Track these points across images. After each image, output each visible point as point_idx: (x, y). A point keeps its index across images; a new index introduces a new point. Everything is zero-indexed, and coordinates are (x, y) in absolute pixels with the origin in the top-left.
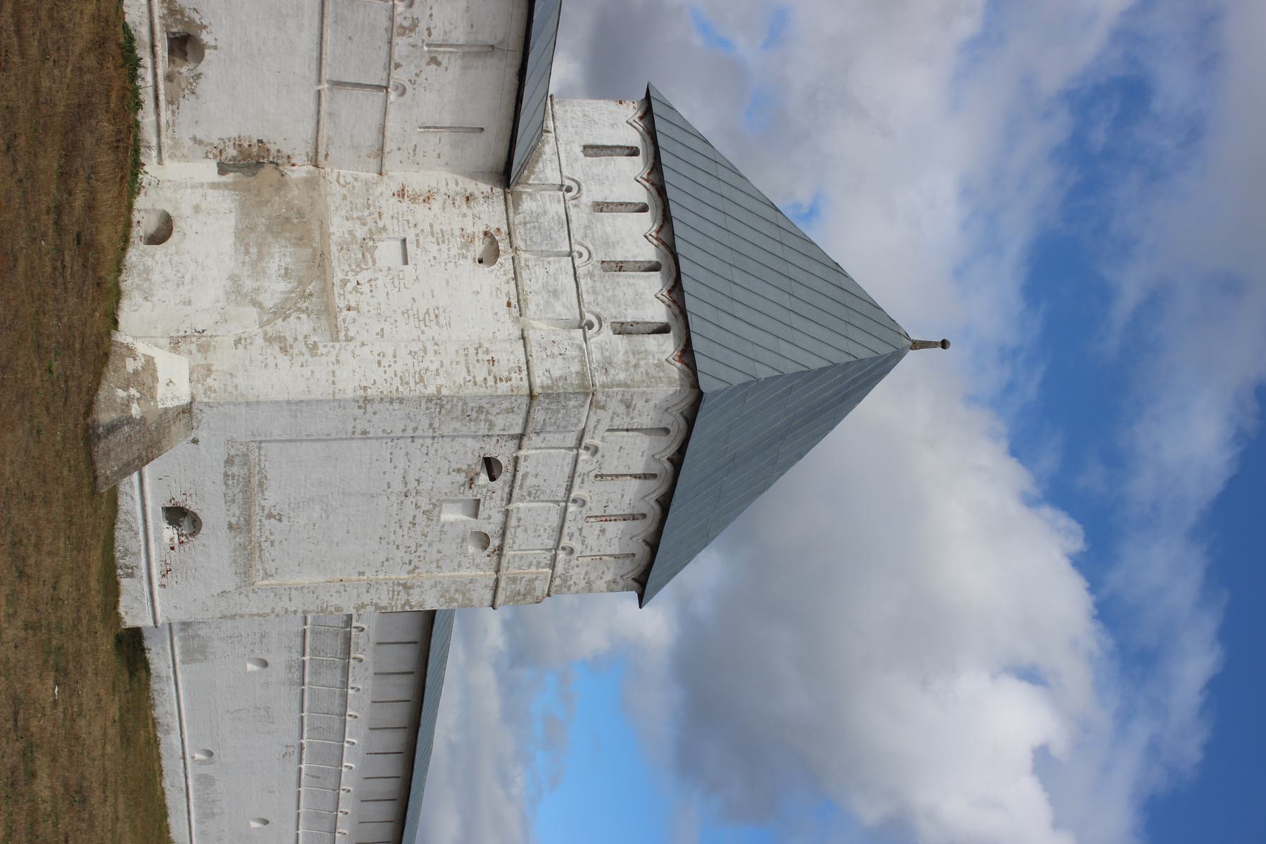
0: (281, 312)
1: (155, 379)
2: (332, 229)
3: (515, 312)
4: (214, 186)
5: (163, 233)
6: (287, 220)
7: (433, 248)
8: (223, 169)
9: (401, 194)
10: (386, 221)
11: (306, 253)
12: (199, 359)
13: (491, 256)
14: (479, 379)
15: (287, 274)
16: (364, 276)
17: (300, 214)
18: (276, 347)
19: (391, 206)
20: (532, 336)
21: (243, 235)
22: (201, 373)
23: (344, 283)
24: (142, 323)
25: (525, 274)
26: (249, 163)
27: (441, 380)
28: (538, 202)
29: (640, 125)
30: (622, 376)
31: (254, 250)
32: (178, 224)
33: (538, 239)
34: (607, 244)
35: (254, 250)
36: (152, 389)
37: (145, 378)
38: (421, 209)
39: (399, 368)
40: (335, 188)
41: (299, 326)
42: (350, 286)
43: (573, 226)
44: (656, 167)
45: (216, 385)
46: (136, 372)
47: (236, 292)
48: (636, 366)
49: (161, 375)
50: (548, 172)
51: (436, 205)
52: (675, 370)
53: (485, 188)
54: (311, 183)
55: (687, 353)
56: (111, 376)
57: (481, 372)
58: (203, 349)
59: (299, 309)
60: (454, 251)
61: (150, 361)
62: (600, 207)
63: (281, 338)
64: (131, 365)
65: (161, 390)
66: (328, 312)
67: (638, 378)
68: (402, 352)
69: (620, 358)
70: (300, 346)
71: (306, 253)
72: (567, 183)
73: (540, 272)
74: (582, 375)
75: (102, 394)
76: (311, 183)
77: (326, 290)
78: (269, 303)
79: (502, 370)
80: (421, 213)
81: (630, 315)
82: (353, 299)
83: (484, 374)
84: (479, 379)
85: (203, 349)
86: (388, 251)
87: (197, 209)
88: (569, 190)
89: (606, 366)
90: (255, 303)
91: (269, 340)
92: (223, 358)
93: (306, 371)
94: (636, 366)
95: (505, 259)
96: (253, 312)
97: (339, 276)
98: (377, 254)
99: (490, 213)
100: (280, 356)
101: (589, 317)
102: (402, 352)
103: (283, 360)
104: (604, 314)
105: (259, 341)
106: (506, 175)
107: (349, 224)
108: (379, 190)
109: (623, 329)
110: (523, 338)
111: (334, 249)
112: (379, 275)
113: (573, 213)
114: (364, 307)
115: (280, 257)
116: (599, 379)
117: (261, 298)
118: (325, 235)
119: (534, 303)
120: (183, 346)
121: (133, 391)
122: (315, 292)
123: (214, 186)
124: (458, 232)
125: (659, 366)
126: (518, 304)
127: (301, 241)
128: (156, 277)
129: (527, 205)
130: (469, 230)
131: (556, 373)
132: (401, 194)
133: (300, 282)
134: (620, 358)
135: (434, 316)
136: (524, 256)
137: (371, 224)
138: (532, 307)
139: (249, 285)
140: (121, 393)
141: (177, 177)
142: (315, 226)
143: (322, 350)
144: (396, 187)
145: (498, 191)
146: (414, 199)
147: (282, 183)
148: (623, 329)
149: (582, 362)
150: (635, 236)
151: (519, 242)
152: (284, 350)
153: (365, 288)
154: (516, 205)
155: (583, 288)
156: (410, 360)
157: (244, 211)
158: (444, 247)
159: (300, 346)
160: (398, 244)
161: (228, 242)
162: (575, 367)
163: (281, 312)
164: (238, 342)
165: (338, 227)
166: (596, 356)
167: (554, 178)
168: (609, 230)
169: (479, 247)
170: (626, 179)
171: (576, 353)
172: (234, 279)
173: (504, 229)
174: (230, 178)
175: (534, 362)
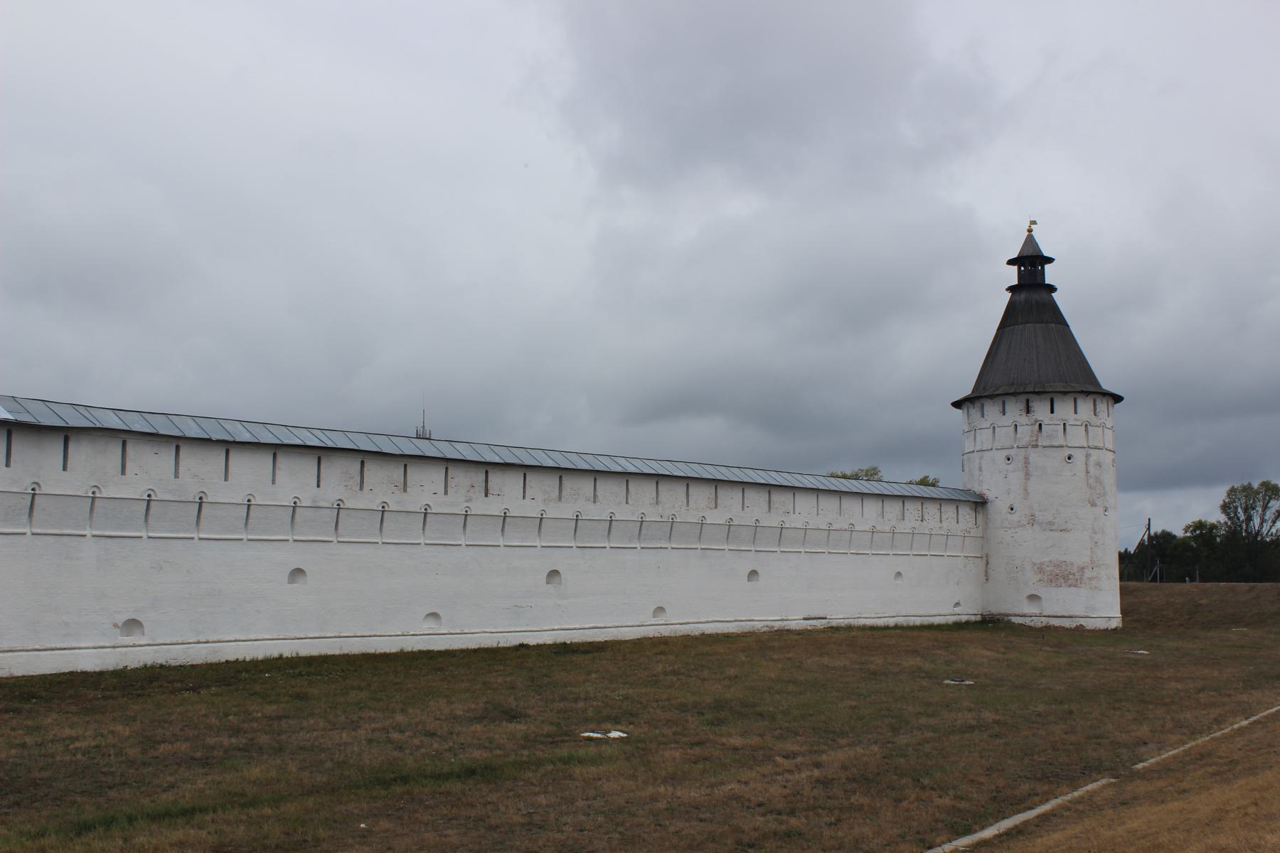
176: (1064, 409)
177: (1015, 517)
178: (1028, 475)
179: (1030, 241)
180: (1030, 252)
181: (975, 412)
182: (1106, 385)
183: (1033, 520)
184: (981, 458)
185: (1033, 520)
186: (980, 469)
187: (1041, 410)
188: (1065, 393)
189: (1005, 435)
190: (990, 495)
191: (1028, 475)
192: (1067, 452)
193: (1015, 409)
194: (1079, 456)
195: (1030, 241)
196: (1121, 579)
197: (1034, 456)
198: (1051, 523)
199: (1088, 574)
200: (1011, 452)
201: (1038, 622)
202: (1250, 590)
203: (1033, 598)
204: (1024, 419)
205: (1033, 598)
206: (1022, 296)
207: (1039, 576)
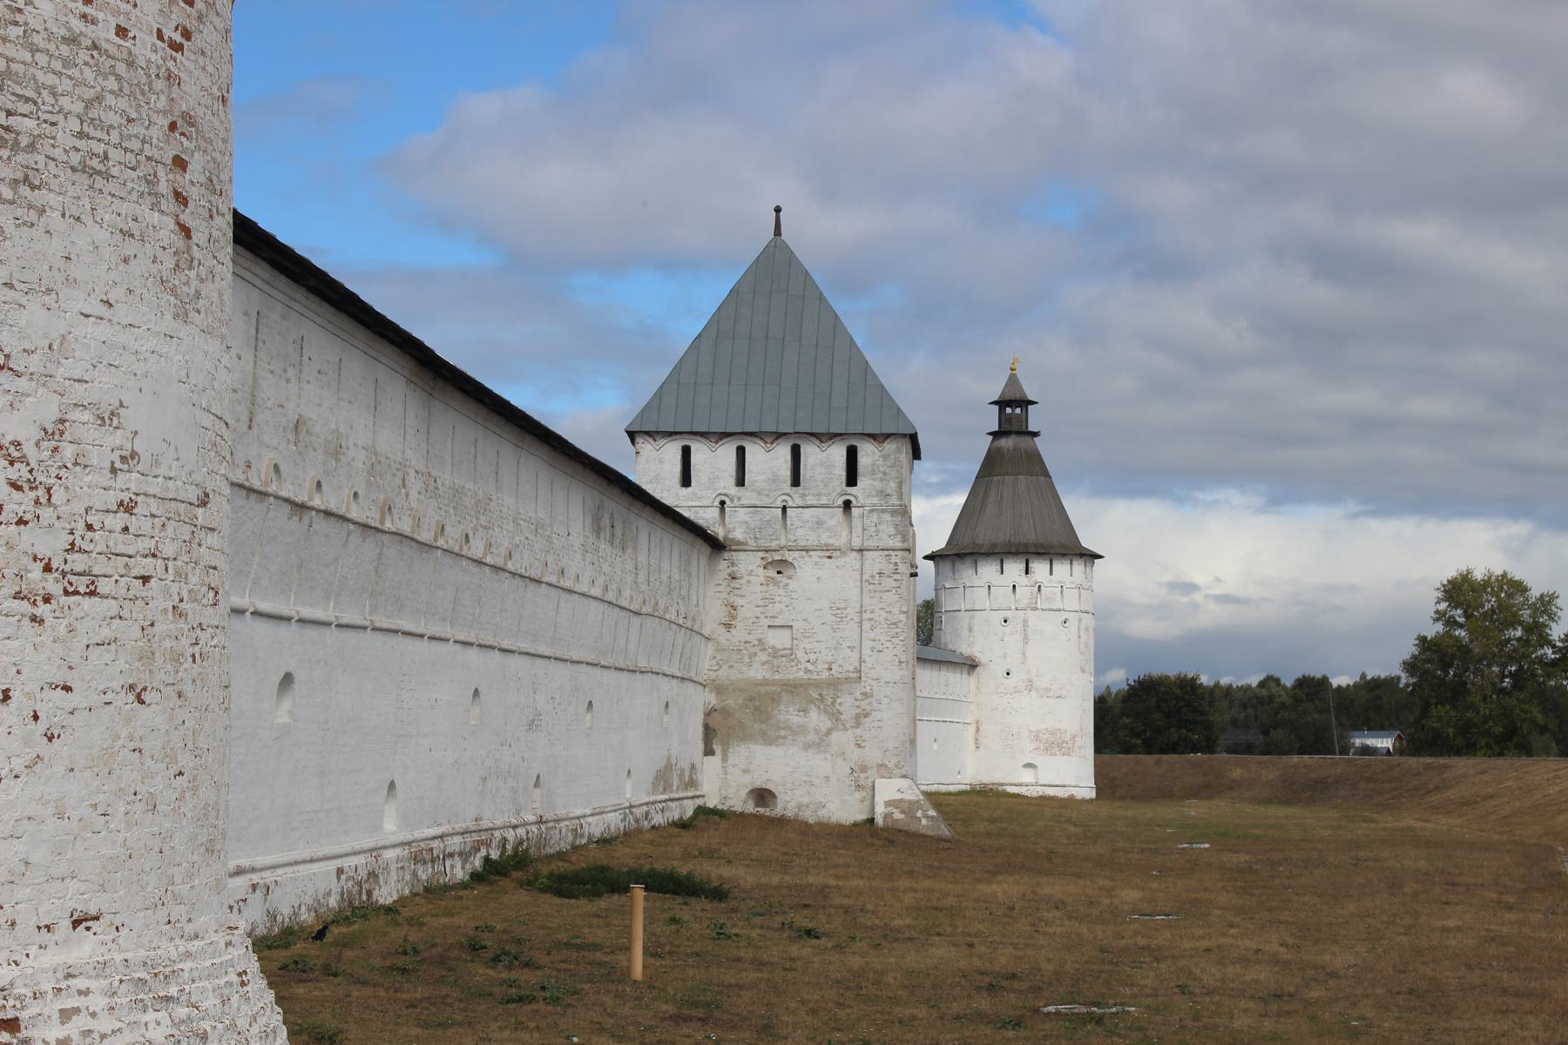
0: (836, 716)
1: (901, 801)
2: (760, 677)
3: (835, 554)
4: (725, 758)
5: (763, 796)
6: (756, 708)
7: (778, 607)
8: (709, 751)
9: (728, 626)
10: (753, 639)
11: (784, 696)
12: (872, 773)
13: (781, 566)
14: (896, 584)
15: (805, 711)
16: (801, 656)
17: (752, 699)
18: (863, 720)
19: (738, 634)
20: (856, 543)
21: (768, 740)
22: (884, 771)
23: (807, 671)
24: (843, 809)
25: (802, 543)
26: (709, 733)
27: (896, 610)
28: (736, 526)
29: (662, 442)
30: (893, 485)
31: (782, 733)
32: (759, 784)
33: (770, 531)
34: (775, 479)
35: (782, 733)
36: (910, 802)
37: (909, 808)
38: (741, 613)
39: (884, 639)
40: (721, 673)
41: (847, 704)
42: (810, 667)
43: (758, 503)
44: (704, 435)
45: (894, 761)
46: (903, 812)
47: (820, 744)
48: (885, 473)
49: (898, 796)
50: (706, 516)
51: (738, 601)
52: (890, 446)
53: (723, 565)
54: (720, 689)
55: (878, 438)
56: (913, 827)
57: (890, 583)
58: (864, 769)
59: (833, 703)
60: (781, 592)
61: (888, 804)
62: (740, 481)
63: (857, 717)
64: (898, 815)
65: (908, 796)
66: (835, 684)
67: (894, 474)
68: (872, 635)
69: (877, 484)
70: (864, 704)
71: (784, 696)
72: (717, 503)
73: (800, 532)
74: (894, 513)
75: (930, 833)
76: (720, 689)
77: (817, 684)
78: (829, 724)
79: (888, 568)
80: (747, 611)
81: (841, 470)
82: (822, 666)
83: (891, 581)
84: (896, 584)
85: (864, 769)
86: (778, 639)
87: (746, 771)
88: (723, 503)
89: (883, 494)
90: (829, 732)
91: (858, 725)
92: (873, 755)
93: (885, 701)
94: (885, 473)
95: (789, 556)
96: (835, 735)
97: (801, 673)
98: (779, 646)
99: (748, 563)
100: (871, 718)
101: (840, 502)
102: (872, 635)
103: (875, 716)
104: (839, 490)
105: (859, 732)
106: (716, 546)
107: (755, 665)
108: (723, 640)
109: (852, 479)
110: (861, 550)
111: (777, 677)
112: (801, 646)
113: (745, 502)
114: (830, 658)
115: (789, 714)
116: (894, 500)
117: (824, 730)
118: (765, 682)
119: (825, 538)
120: (862, 782)
121: (919, 814)
122: (820, 692)
123: (725, 758)
124: (764, 588)
125: (885, 457)
126: (829, 551)
127: (775, 699)
128: (805, 800)
129: (738, 534)
130: (762, 579)
131: (892, 531)
132: (728, 626)
133: (811, 702)
134: (877, 484)
135: (838, 612)
136: (783, 542)
137: (755, 649)
138: (831, 541)
139: (812, 737)
140: (924, 822)
141: (722, 783)
142: (762, 689)
143: (868, 689)
144: (722, 630)
145: (726, 555)
146: (734, 618)
147: (725, 712)
148: (852, 479)
149: (883, 511)
150: (768, 461)
151: (774, 545)
152: (867, 715)
153: (812, 657)
154: (739, 543)
155: (815, 502)
156: (877, 631)
157: (747, 737)
158: (778, 599)
159: (864, 704)
160: (771, 631)
161: (775, 751)
162: (887, 517)
163: (836, 716)
164: (859, 746)
165: (758, 672)
166: (875, 500)
167: (715, 512)
168: (762, 478)
169: (772, 573)
170: (713, 461)
171: (874, 518)
172: (807, 747)
173: (762, 554)
174: (717, 748)
175: (882, 545)
176: (1062, 568)
177: (1011, 682)
178: (1026, 639)
179: (1013, 380)
180: (1011, 396)
181: (946, 567)
182: (1087, 542)
183: (1030, 686)
184: (972, 618)
185: (1030, 686)
186: (970, 630)
187: (1040, 568)
188: (1064, 555)
189: (1002, 594)
190: (980, 657)
191: (1026, 639)
192: (1064, 615)
193: (1014, 568)
194: (1073, 618)
195: (1013, 380)
196: (1100, 746)
197: (1033, 617)
198: (1047, 689)
199: (1079, 742)
200: (1008, 614)
201: (1033, 792)
202: (1158, 763)
203: (1029, 765)
204: (1022, 580)
205: (1029, 765)
206: (1006, 443)
207: (1035, 744)
